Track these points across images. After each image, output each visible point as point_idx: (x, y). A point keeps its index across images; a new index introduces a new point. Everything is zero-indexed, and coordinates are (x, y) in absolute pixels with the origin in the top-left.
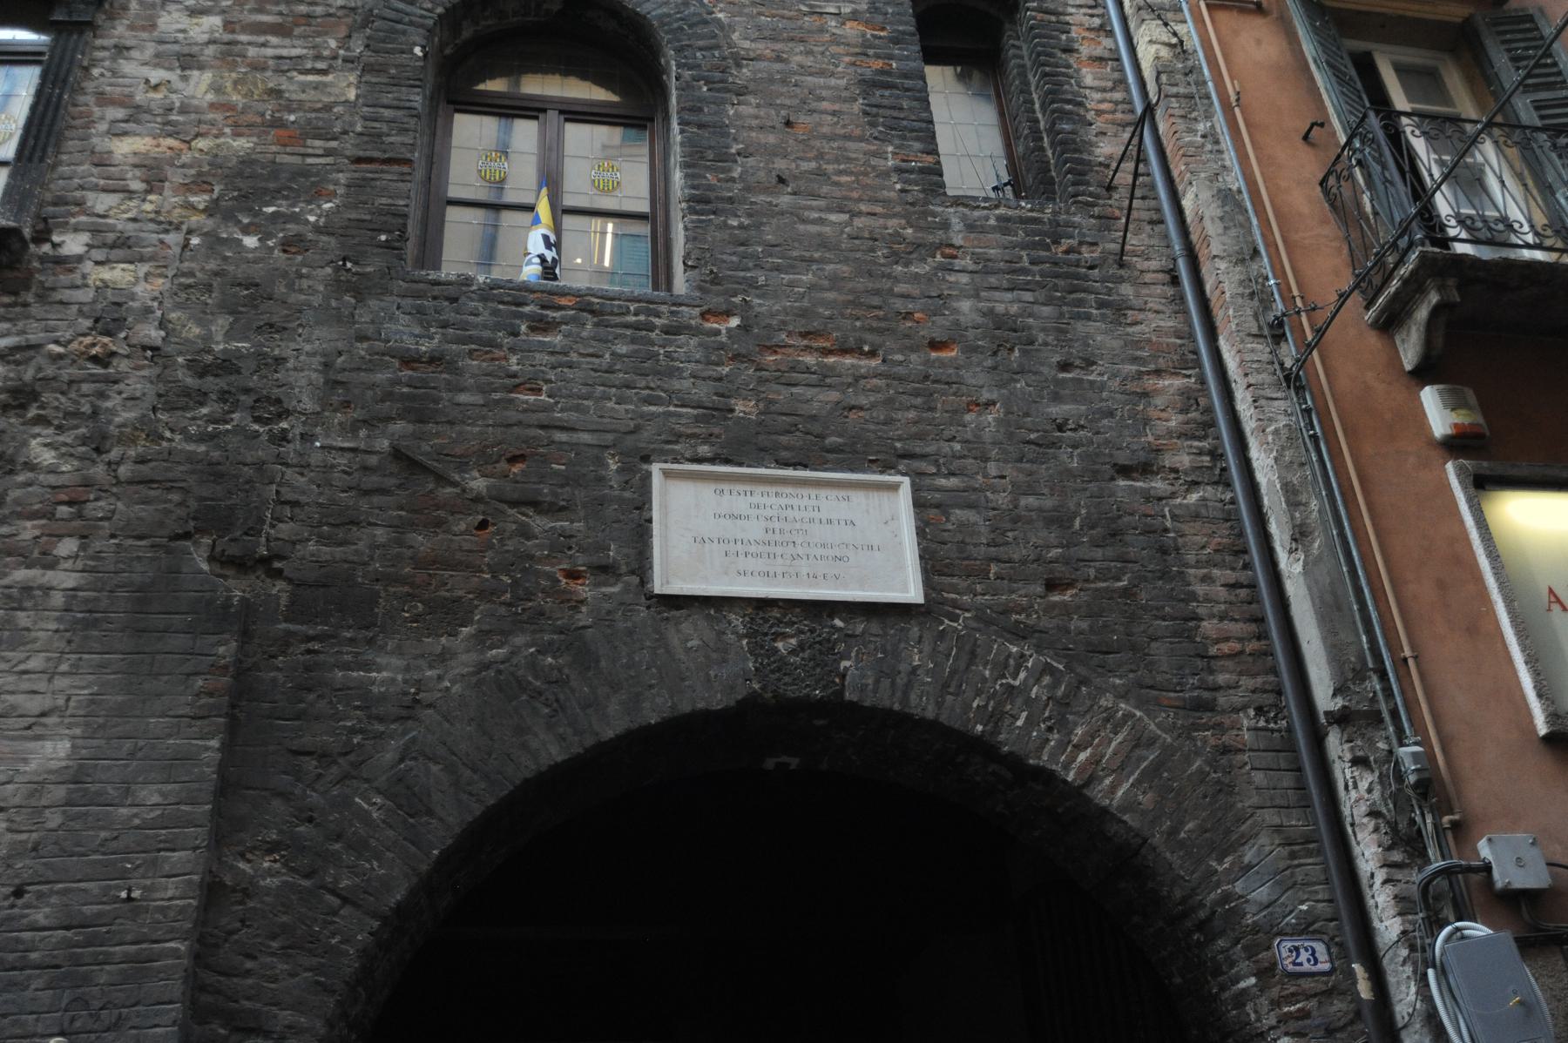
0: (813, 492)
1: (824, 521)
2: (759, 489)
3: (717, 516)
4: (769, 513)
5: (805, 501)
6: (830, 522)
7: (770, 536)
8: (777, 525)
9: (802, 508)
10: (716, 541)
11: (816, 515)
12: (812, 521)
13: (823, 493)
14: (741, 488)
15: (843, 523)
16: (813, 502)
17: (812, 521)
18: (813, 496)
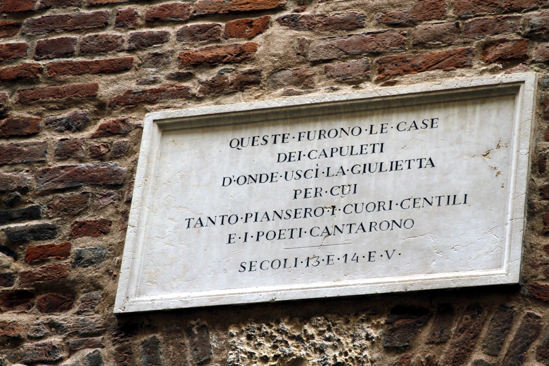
0: (376, 121)
1: (386, 166)
2: (293, 131)
3: (227, 181)
4: (306, 164)
5: (357, 141)
6: (395, 166)
7: (301, 203)
8: (311, 183)
9: (357, 150)
10: (218, 221)
11: (370, 158)
12: (368, 168)
13: (394, 119)
14: (269, 132)
15: (415, 165)
16: (377, 138)
17: (368, 168)
18: (377, 128)
